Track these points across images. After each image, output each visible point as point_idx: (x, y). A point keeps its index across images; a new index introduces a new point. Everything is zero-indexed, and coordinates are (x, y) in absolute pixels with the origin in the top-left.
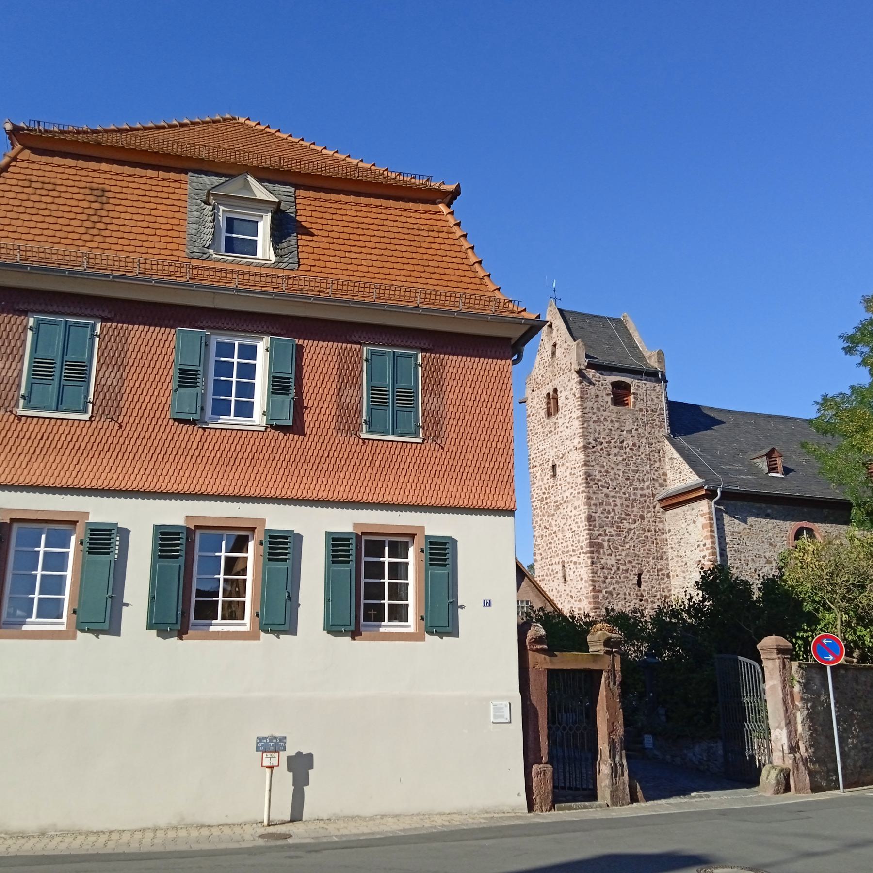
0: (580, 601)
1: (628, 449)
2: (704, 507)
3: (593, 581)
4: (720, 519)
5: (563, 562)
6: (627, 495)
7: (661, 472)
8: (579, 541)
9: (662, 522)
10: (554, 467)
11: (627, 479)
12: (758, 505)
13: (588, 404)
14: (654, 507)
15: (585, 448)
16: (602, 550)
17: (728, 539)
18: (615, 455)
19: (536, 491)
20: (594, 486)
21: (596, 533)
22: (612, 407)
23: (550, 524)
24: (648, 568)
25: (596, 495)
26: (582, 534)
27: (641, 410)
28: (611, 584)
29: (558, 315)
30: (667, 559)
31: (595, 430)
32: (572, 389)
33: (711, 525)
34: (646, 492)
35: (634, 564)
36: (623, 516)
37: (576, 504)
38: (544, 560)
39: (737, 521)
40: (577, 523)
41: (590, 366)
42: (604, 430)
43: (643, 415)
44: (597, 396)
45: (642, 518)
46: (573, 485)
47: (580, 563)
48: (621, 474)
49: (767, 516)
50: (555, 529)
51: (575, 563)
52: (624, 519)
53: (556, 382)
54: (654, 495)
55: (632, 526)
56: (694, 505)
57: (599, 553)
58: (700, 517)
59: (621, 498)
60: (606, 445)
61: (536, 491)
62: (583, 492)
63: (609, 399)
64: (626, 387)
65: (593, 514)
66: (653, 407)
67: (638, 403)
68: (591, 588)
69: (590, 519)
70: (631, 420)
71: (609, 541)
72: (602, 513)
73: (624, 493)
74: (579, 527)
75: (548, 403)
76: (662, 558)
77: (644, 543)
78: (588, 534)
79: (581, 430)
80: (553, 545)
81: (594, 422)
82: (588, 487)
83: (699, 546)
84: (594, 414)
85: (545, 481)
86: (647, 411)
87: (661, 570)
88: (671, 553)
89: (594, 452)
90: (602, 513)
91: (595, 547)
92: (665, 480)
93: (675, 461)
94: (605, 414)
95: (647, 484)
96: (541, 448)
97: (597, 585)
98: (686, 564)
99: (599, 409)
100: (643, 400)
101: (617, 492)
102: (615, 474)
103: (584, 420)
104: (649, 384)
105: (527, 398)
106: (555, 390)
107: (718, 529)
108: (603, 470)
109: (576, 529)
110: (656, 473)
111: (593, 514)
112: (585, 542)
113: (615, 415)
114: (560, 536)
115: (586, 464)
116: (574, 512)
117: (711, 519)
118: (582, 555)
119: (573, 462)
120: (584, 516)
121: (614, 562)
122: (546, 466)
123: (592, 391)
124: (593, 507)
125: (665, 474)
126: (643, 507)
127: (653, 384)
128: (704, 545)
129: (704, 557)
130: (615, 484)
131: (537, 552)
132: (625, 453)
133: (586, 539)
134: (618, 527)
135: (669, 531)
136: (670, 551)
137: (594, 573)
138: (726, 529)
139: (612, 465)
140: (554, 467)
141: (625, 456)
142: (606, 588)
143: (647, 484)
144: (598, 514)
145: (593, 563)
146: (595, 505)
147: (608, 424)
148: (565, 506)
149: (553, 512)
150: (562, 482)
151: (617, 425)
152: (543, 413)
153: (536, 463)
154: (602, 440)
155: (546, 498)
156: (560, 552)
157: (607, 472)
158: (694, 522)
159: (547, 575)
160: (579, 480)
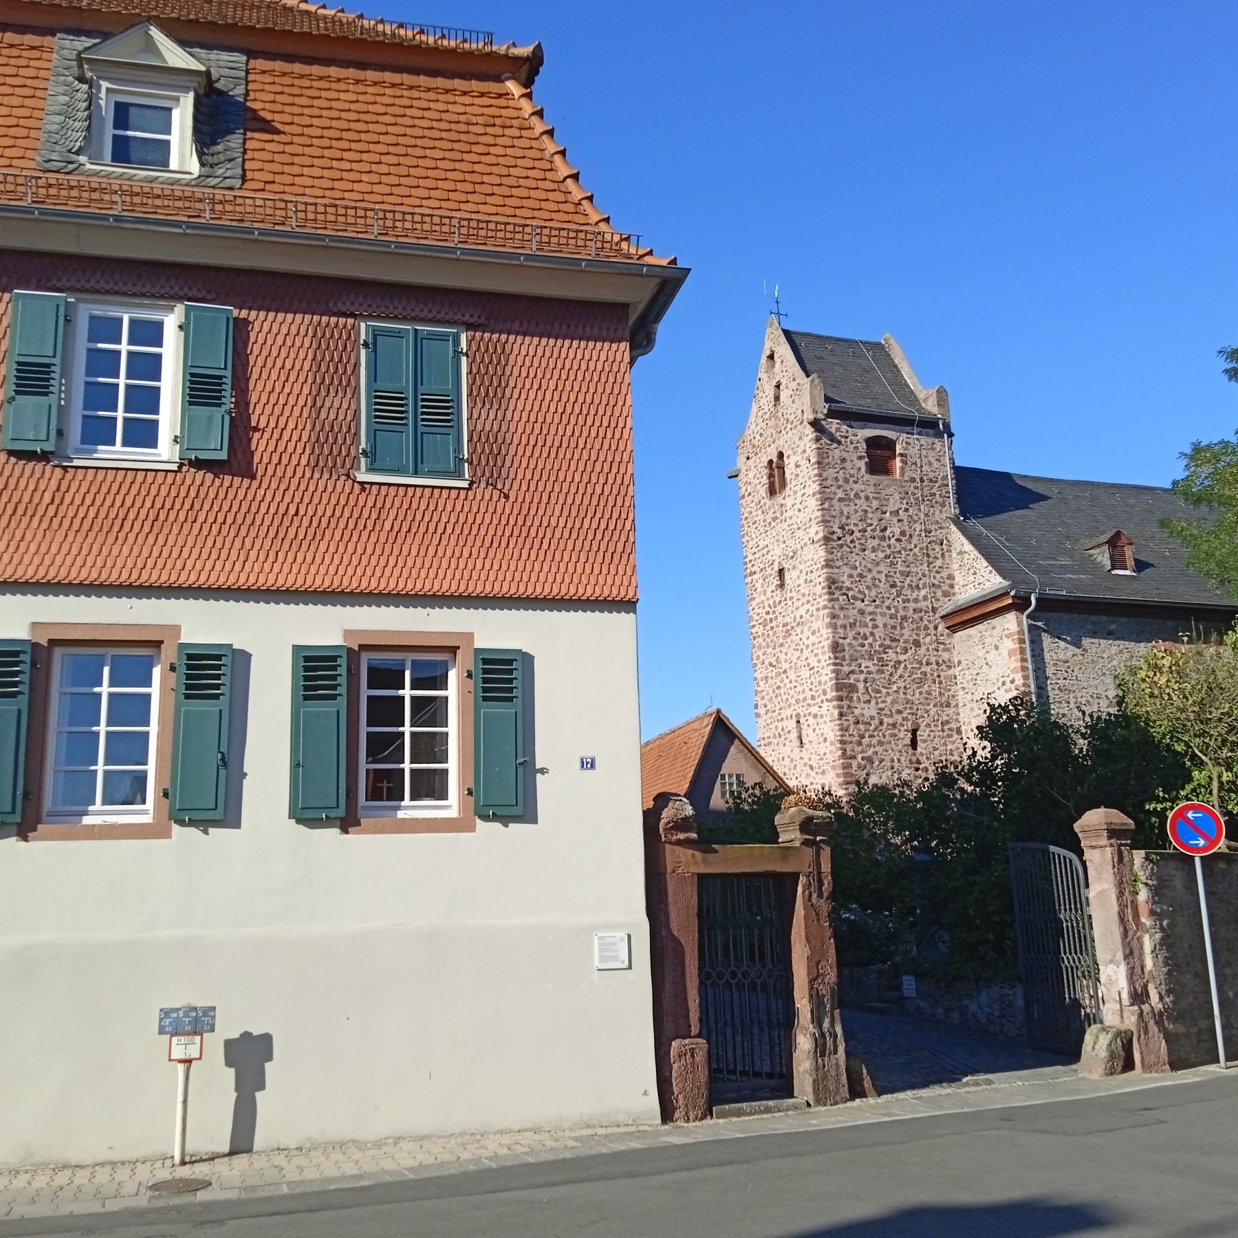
0: (823, 773)
1: (893, 541)
2: (1011, 623)
3: (841, 742)
4: (1036, 643)
5: (798, 715)
6: (893, 611)
7: (945, 574)
8: (820, 683)
9: (947, 650)
10: (781, 572)
11: (893, 586)
12: (1094, 618)
13: (830, 473)
14: (936, 628)
15: (827, 539)
16: (855, 696)
17: (1050, 671)
18: (874, 550)
19: (757, 610)
20: (841, 598)
21: (846, 669)
22: (867, 477)
23: (778, 660)
24: (927, 721)
25: (845, 612)
26: (824, 672)
27: (913, 480)
28: (870, 746)
29: (783, 339)
30: (957, 706)
31: (842, 513)
32: (804, 451)
33: (1022, 651)
34: (922, 605)
35: (905, 715)
36: (888, 642)
37: (815, 626)
38: (770, 714)
39: (1062, 644)
40: (816, 655)
41: (832, 414)
42: (856, 511)
43: (916, 488)
44: (843, 460)
45: (917, 644)
46: (811, 599)
47: (822, 716)
48: (883, 579)
49: (1110, 635)
50: (785, 666)
51: (815, 716)
52: (889, 647)
53: (781, 442)
54: (934, 610)
55: (902, 658)
56: (997, 621)
57: (851, 699)
58: (1005, 640)
59: (883, 615)
60: (859, 535)
61: (757, 610)
62: (825, 607)
63: (862, 464)
64: (890, 445)
65: (841, 641)
66: (931, 475)
67: (907, 468)
68: (840, 753)
69: (836, 648)
70: (897, 496)
71: (865, 681)
72: (855, 638)
73: (889, 608)
74: (819, 661)
75: (771, 476)
76: (948, 705)
77: (921, 682)
78: (833, 671)
79: (819, 513)
80: (782, 691)
81: (840, 500)
82: (832, 600)
83: (1004, 683)
84: (839, 487)
85: (769, 594)
86: (922, 481)
87: (947, 722)
88: (962, 697)
89: (841, 546)
90: (855, 638)
91: (844, 690)
92: (952, 586)
93: (966, 556)
94: (856, 487)
95: (923, 592)
96: (762, 544)
97: (849, 747)
99: (846, 481)
100: (915, 464)
101: (876, 607)
102: (874, 579)
103: (825, 497)
104: (924, 440)
105: (739, 470)
106: (781, 455)
107: (1033, 656)
108: (855, 573)
109: (816, 664)
110: (938, 576)
111: (841, 641)
112: (830, 684)
113: (872, 489)
114: (792, 676)
115: (828, 564)
116: (813, 639)
117: (1022, 641)
118: (825, 704)
119: (809, 563)
120: (827, 644)
121: (874, 712)
122: (769, 570)
123: (836, 453)
124: (841, 631)
125: (951, 577)
126: (918, 628)
127: (930, 440)
128: (1012, 682)
130: (873, 593)
131: (760, 702)
132: (889, 546)
133: (831, 679)
134: (880, 659)
135: (959, 662)
136: (961, 693)
137: (844, 729)
138: (1047, 656)
139: (869, 566)
140: (781, 572)
141: (888, 552)
142: (863, 752)
143: (923, 592)
144: (848, 641)
145: (841, 715)
146: (844, 627)
147: (862, 503)
148: (799, 630)
150: (794, 594)
151: (875, 504)
152: (763, 491)
153: (755, 569)
154: (852, 527)
155: (771, 620)
156: (793, 701)
157: (861, 576)
158: (997, 648)
159: (775, 737)
160: (819, 590)
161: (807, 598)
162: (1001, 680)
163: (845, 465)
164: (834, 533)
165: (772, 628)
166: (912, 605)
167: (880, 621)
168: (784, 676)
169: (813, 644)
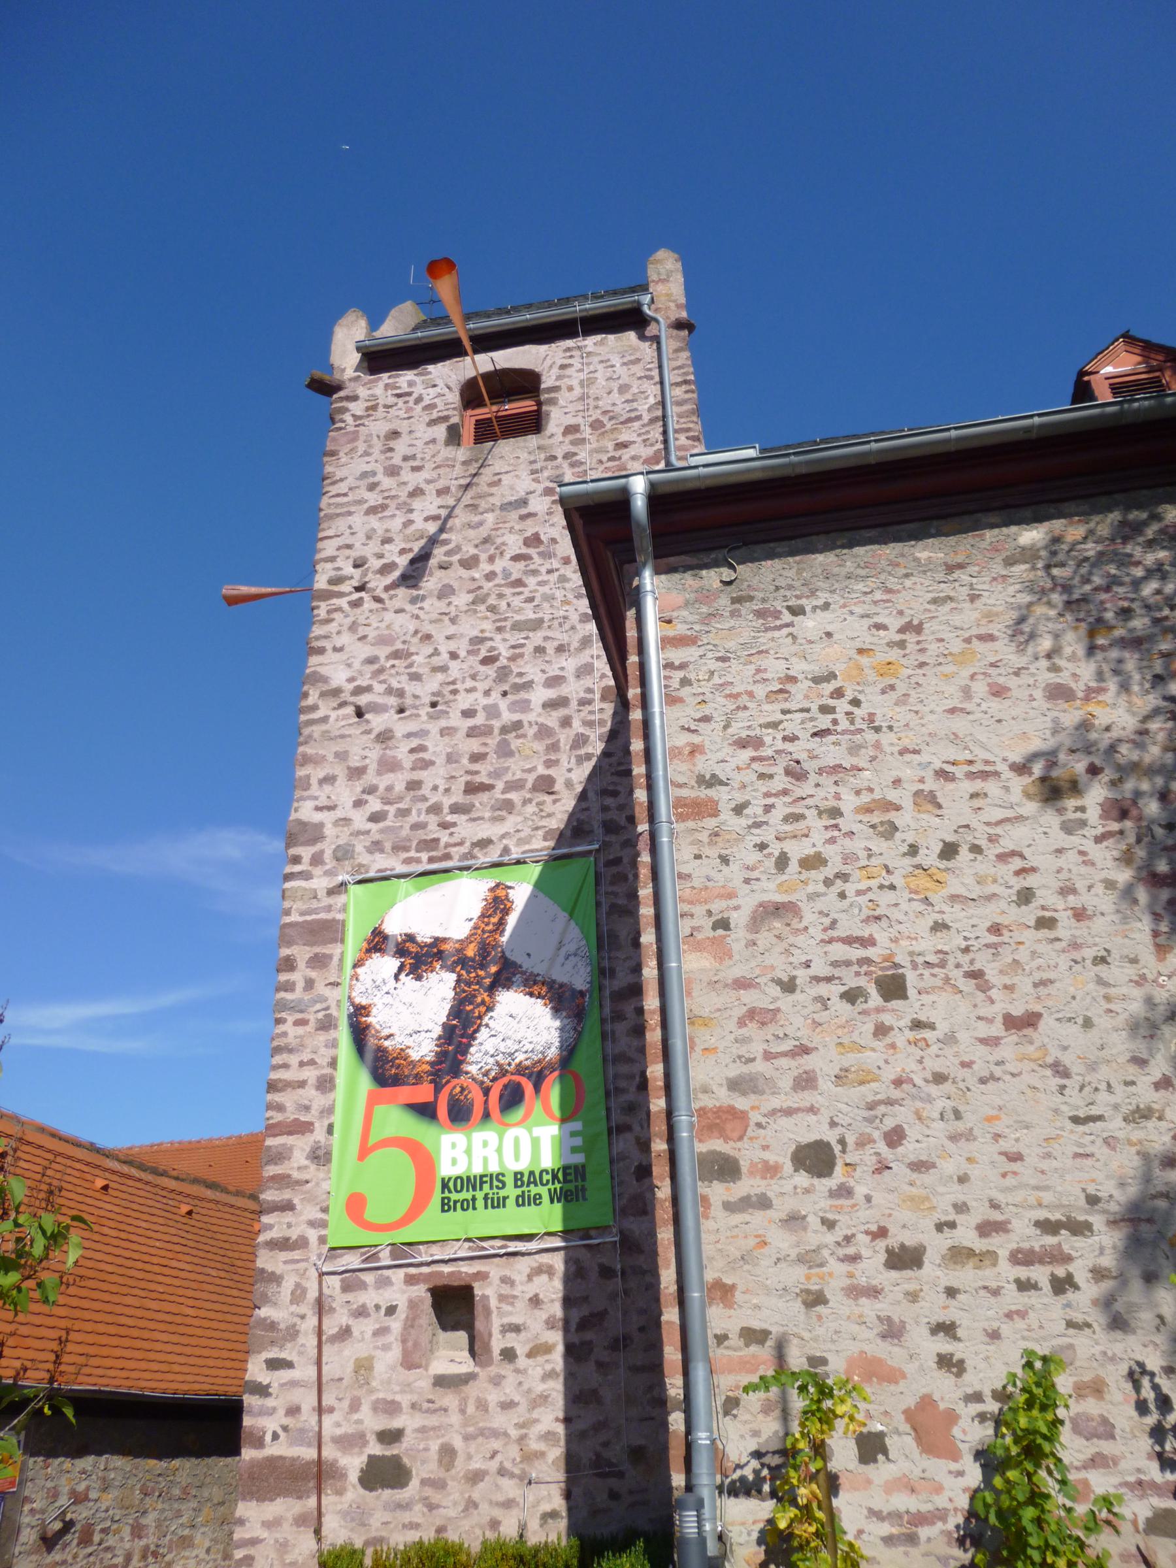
113: (458, 470)
139: (427, 628)
163: (392, 444)
166: (539, 695)
167: (436, 747)
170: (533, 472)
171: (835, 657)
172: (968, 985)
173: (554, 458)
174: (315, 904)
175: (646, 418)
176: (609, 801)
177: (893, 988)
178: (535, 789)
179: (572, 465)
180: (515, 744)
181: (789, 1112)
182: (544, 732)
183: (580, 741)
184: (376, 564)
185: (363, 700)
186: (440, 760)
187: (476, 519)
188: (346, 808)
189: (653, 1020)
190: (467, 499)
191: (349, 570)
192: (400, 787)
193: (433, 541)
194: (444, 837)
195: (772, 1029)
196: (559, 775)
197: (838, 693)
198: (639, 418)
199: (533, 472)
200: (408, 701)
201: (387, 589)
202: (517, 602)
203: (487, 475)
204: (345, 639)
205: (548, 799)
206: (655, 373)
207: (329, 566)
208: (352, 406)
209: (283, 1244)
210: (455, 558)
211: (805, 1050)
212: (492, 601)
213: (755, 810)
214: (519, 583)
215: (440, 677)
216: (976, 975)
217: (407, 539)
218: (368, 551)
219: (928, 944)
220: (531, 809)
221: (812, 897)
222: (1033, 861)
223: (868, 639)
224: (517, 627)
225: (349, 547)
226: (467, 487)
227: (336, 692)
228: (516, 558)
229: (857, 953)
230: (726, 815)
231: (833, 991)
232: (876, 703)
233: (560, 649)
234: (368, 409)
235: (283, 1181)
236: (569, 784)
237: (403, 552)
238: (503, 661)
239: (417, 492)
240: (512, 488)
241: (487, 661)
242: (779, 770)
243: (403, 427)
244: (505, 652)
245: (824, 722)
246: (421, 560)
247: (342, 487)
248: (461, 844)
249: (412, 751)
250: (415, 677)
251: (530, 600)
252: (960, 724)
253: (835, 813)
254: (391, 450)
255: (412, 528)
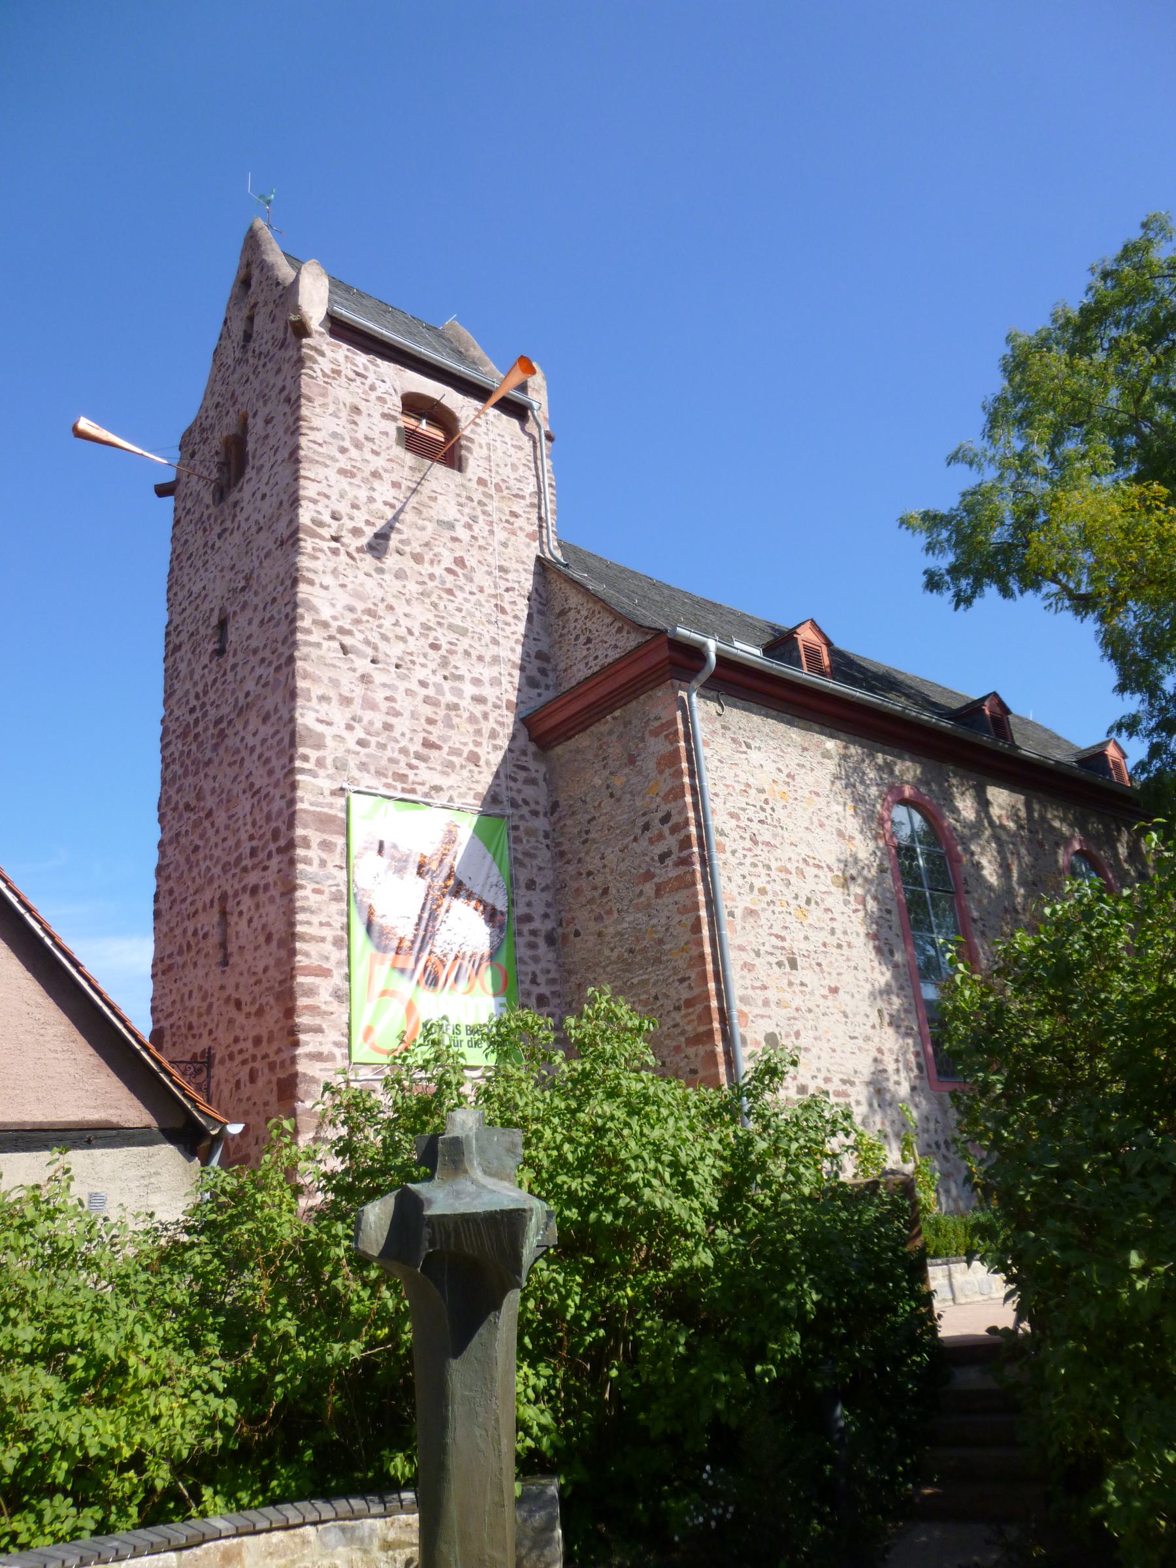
0: (260, 1012)
5: (224, 898)
8: (268, 818)
10: (223, 624)
20: (326, 644)
23: (200, 797)
37: (269, 705)
38: (176, 909)
44: (356, 410)
46: (267, 654)
47: (266, 888)
51: (254, 890)
80: (201, 855)
83: (646, 827)
90: (349, 727)
96: (196, 589)
98: (605, 891)
109: (265, 781)
113: (407, 472)
114: (221, 818)
122: (202, 631)
129: (663, 857)
139: (391, 600)
140: (223, 624)
149: (209, 754)
155: (197, 721)
156: (216, 871)
159: (180, 953)
161: (260, 655)
162: (641, 822)
163: (356, 418)
164: (321, 524)
165: (197, 736)
166: (469, 690)
167: (403, 703)
168: (207, 824)
169: (264, 741)
170: (460, 505)
171: (762, 779)
172: (817, 968)
173: (471, 500)
174: (321, 799)
175: (528, 500)
176: (512, 784)
177: (793, 964)
178: (468, 759)
179: (484, 513)
180: (456, 720)
181: (762, 1017)
182: (472, 719)
183: (493, 735)
184: (350, 525)
185: (347, 641)
186: (407, 714)
187: (420, 522)
188: (339, 728)
189: (709, 959)
190: (414, 500)
191: (326, 518)
192: (378, 725)
193: (391, 526)
194: (411, 774)
195: (753, 974)
196: (482, 752)
197: (766, 801)
198: (523, 497)
199: (460, 505)
200: (381, 657)
201: (360, 550)
202: (451, 607)
203: (426, 489)
204: (328, 580)
205: (476, 769)
206: (532, 465)
207: (311, 505)
208: (319, 359)
209: (318, 1057)
210: (407, 549)
211: (765, 988)
212: (434, 598)
213: (739, 854)
214: (450, 592)
215: (401, 645)
216: (819, 965)
217: (370, 512)
218: (343, 508)
219: (804, 946)
220: (465, 773)
221: (764, 910)
222: (835, 915)
223: (776, 776)
224: (451, 627)
225: (328, 497)
226: (414, 491)
227: (325, 625)
228: (449, 570)
229: (780, 944)
230: (728, 854)
231: (773, 960)
232: (780, 814)
233: (480, 658)
234: (334, 371)
235: (313, 1010)
236: (488, 763)
237: (368, 523)
238: (443, 652)
239: (375, 474)
240: (444, 509)
241: (435, 647)
242: (747, 836)
243: (363, 406)
244: (445, 646)
245: (762, 816)
246: (382, 537)
247: (318, 437)
248: (422, 784)
249: (387, 699)
250: (385, 638)
251: (459, 610)
252: (809, 836)
253: (769, 868)
254: (355, 423)
255: (374, 506)
